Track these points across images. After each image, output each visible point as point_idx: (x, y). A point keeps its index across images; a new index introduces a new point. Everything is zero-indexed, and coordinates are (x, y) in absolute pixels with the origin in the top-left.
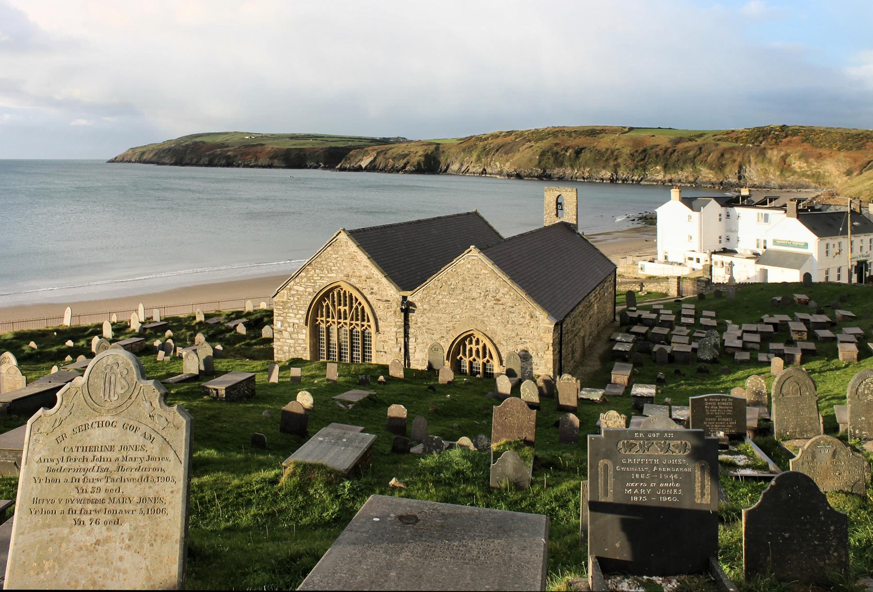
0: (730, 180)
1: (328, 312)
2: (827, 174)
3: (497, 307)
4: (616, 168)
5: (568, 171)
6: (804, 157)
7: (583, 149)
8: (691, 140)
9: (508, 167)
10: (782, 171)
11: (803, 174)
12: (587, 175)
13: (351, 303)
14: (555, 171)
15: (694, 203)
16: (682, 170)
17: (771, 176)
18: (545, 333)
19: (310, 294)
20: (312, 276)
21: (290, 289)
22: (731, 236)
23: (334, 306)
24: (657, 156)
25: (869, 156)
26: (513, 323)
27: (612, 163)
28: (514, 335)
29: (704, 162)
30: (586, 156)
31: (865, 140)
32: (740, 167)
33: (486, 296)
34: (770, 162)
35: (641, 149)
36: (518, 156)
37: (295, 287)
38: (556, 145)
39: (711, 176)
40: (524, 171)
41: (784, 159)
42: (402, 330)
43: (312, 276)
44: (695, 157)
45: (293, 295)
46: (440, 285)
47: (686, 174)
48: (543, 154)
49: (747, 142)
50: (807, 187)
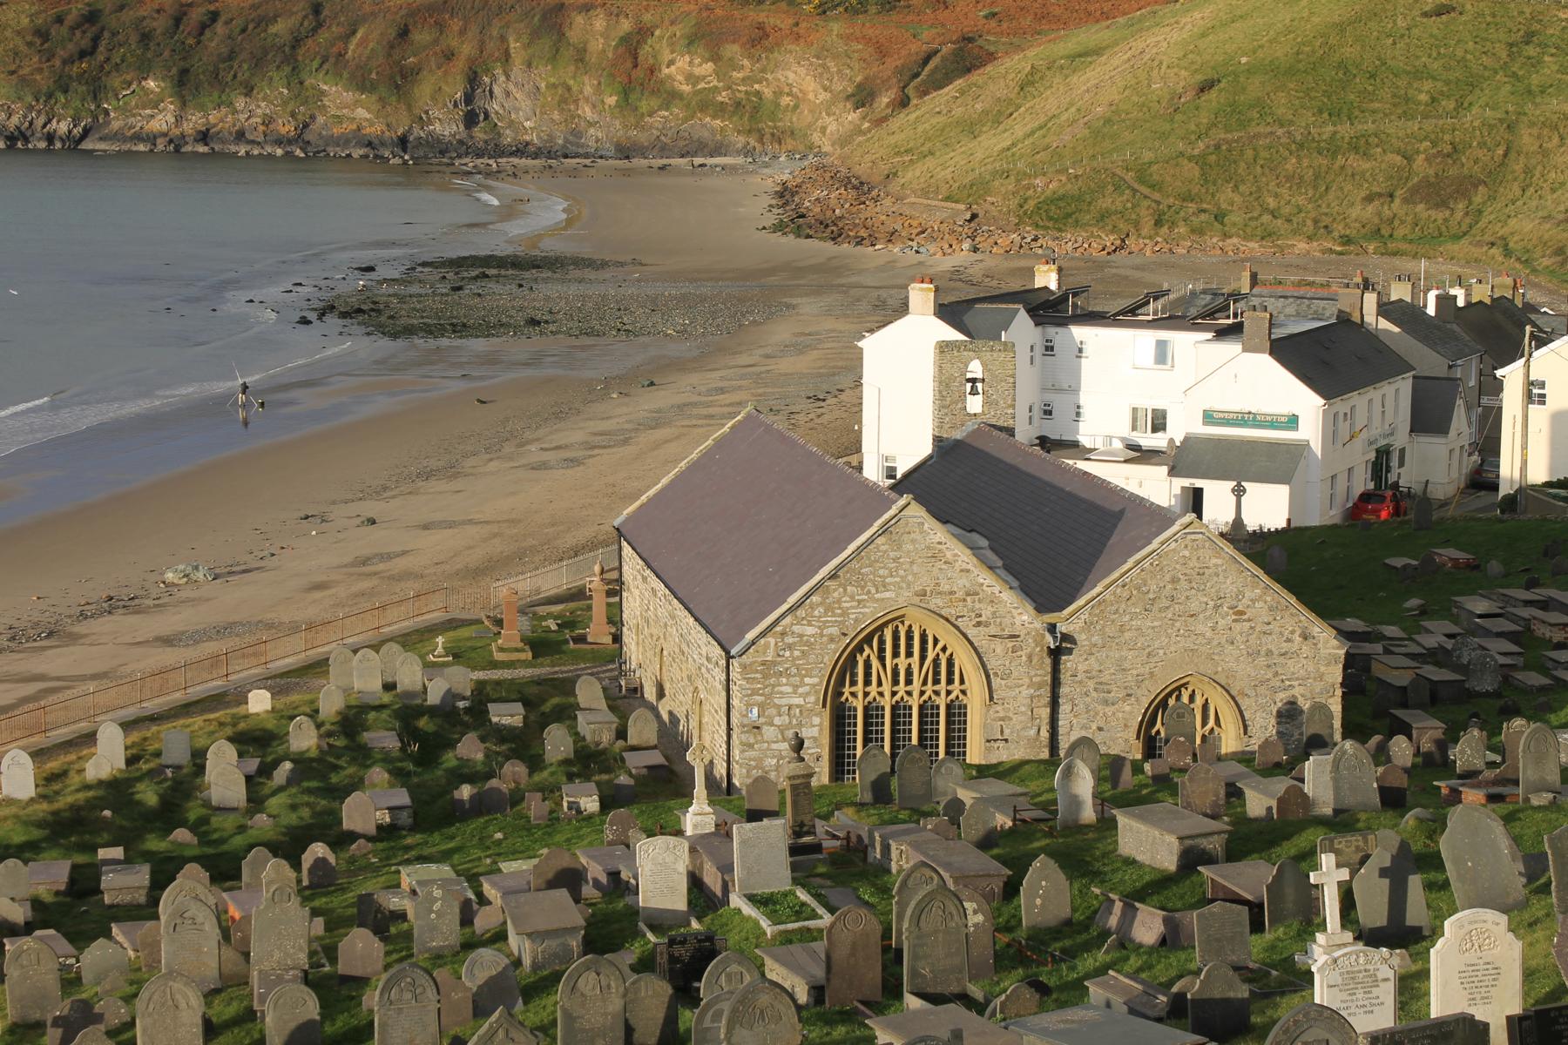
0: (437, 127)
1: (868, 674)
2: (785, 100)
3: (1238, 627)
6: (707, 38)
10: (625, 93)
11: (705, 103)
13: (923, 650)
15: (968, 319)
16: (249, 91)
17: (587, 112)
18: (1328, 664)
19: (832, 640)
20: (839, 601)
21: (783, 634)
22: (1059, 403)
23: (882, 659)
24: (145, 37)
25: (926, 35)
26: (1269, 653)
28: (1270, 675)
29: (334, 62)
32: (473, 80)
33: (1216, 607)
34: (581, 57)
35: (76, 10)
37: (796, 628)
39: (361, 113)
41: (632, 46)
42: (1046, 692)
43: (839, 601)
44: (297, 42)
45: (790, 647)
46: (1126, 594)
47: (263, 108)
50: (718, 150)
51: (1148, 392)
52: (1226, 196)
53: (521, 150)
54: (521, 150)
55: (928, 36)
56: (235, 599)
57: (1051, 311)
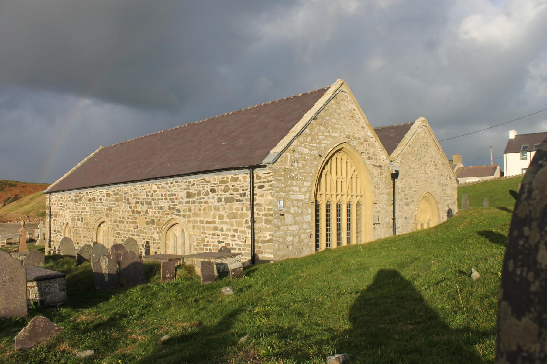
31: (4, 186)
37: (299, 148)
43: (317, 135)
55: (9, 195)
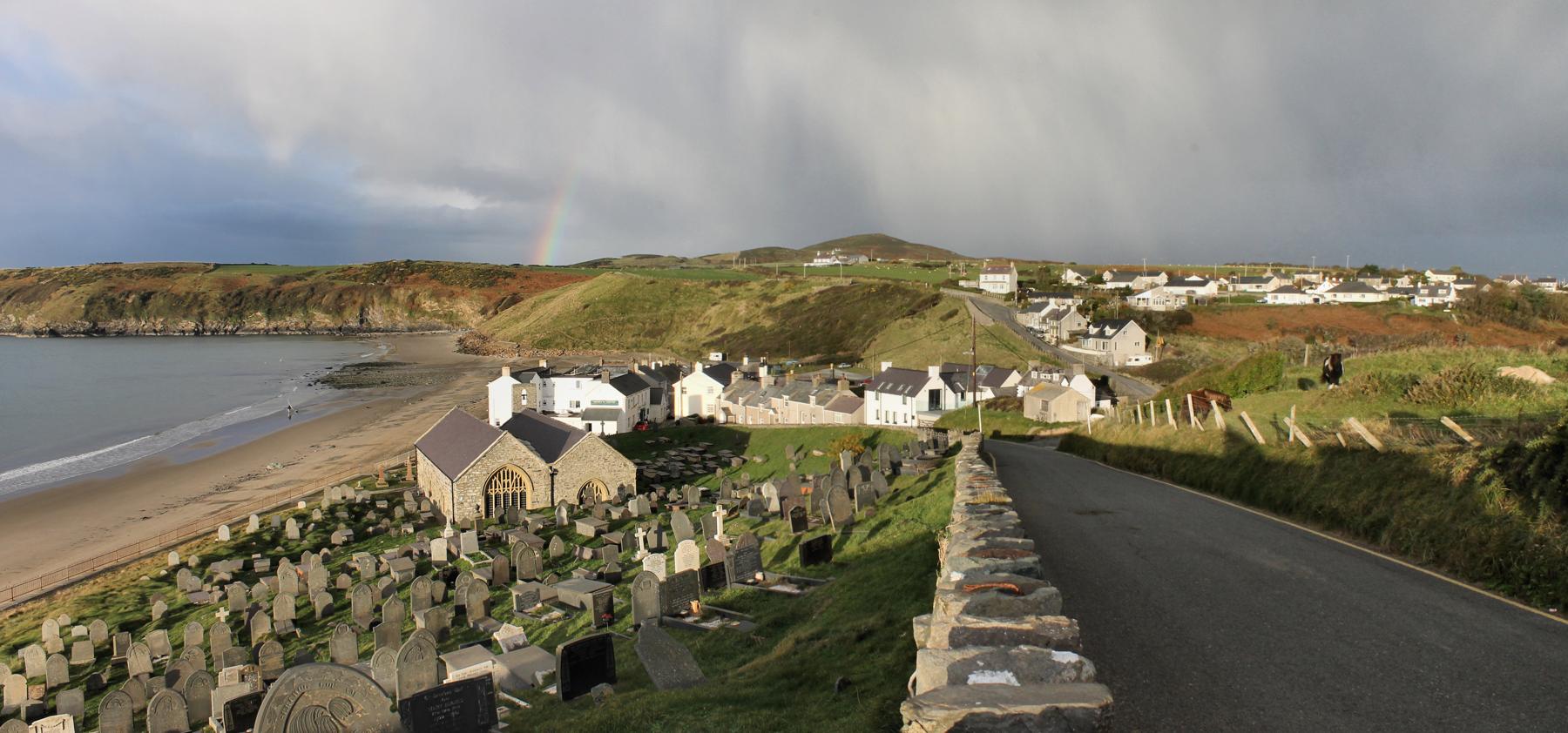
4: (202, 317)
5: (132, 324)
6: (435, 295)
7: (150, 294)
8: (299, 279)
9: (30, 322)
11: (435, 315)
12: (159, 327)
14: (112, 324)
24: (257, 300)
27: (196, 311)
29: (318, 305)
30: (157, 302)
32: (362, 310)
35: (235, 291)
36: (48, 305)
38: (111, 288)
40: (60, 326)
41: (412, 298)
48: (91, 302)
49: (368, 280)
51: (575, 396)
52: (593, 338)
53: (378, 330)
54: (378, 330)
55: (503, 294)
56: (290, 473)
57: (544, 373)
